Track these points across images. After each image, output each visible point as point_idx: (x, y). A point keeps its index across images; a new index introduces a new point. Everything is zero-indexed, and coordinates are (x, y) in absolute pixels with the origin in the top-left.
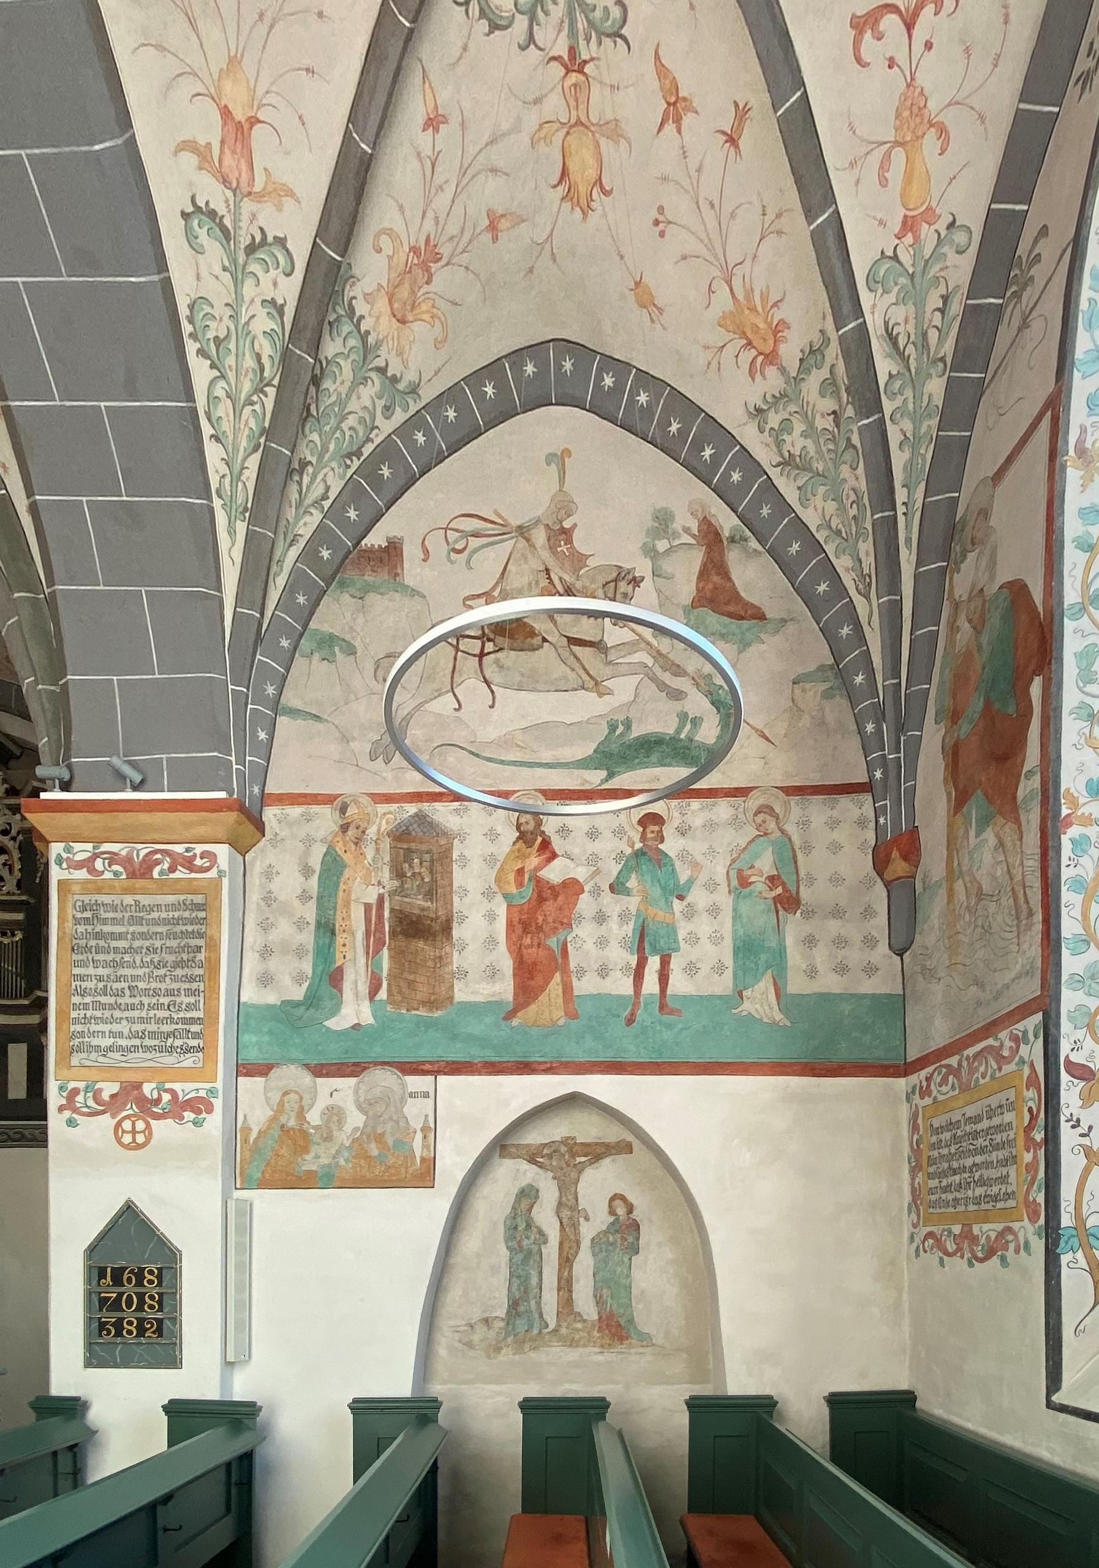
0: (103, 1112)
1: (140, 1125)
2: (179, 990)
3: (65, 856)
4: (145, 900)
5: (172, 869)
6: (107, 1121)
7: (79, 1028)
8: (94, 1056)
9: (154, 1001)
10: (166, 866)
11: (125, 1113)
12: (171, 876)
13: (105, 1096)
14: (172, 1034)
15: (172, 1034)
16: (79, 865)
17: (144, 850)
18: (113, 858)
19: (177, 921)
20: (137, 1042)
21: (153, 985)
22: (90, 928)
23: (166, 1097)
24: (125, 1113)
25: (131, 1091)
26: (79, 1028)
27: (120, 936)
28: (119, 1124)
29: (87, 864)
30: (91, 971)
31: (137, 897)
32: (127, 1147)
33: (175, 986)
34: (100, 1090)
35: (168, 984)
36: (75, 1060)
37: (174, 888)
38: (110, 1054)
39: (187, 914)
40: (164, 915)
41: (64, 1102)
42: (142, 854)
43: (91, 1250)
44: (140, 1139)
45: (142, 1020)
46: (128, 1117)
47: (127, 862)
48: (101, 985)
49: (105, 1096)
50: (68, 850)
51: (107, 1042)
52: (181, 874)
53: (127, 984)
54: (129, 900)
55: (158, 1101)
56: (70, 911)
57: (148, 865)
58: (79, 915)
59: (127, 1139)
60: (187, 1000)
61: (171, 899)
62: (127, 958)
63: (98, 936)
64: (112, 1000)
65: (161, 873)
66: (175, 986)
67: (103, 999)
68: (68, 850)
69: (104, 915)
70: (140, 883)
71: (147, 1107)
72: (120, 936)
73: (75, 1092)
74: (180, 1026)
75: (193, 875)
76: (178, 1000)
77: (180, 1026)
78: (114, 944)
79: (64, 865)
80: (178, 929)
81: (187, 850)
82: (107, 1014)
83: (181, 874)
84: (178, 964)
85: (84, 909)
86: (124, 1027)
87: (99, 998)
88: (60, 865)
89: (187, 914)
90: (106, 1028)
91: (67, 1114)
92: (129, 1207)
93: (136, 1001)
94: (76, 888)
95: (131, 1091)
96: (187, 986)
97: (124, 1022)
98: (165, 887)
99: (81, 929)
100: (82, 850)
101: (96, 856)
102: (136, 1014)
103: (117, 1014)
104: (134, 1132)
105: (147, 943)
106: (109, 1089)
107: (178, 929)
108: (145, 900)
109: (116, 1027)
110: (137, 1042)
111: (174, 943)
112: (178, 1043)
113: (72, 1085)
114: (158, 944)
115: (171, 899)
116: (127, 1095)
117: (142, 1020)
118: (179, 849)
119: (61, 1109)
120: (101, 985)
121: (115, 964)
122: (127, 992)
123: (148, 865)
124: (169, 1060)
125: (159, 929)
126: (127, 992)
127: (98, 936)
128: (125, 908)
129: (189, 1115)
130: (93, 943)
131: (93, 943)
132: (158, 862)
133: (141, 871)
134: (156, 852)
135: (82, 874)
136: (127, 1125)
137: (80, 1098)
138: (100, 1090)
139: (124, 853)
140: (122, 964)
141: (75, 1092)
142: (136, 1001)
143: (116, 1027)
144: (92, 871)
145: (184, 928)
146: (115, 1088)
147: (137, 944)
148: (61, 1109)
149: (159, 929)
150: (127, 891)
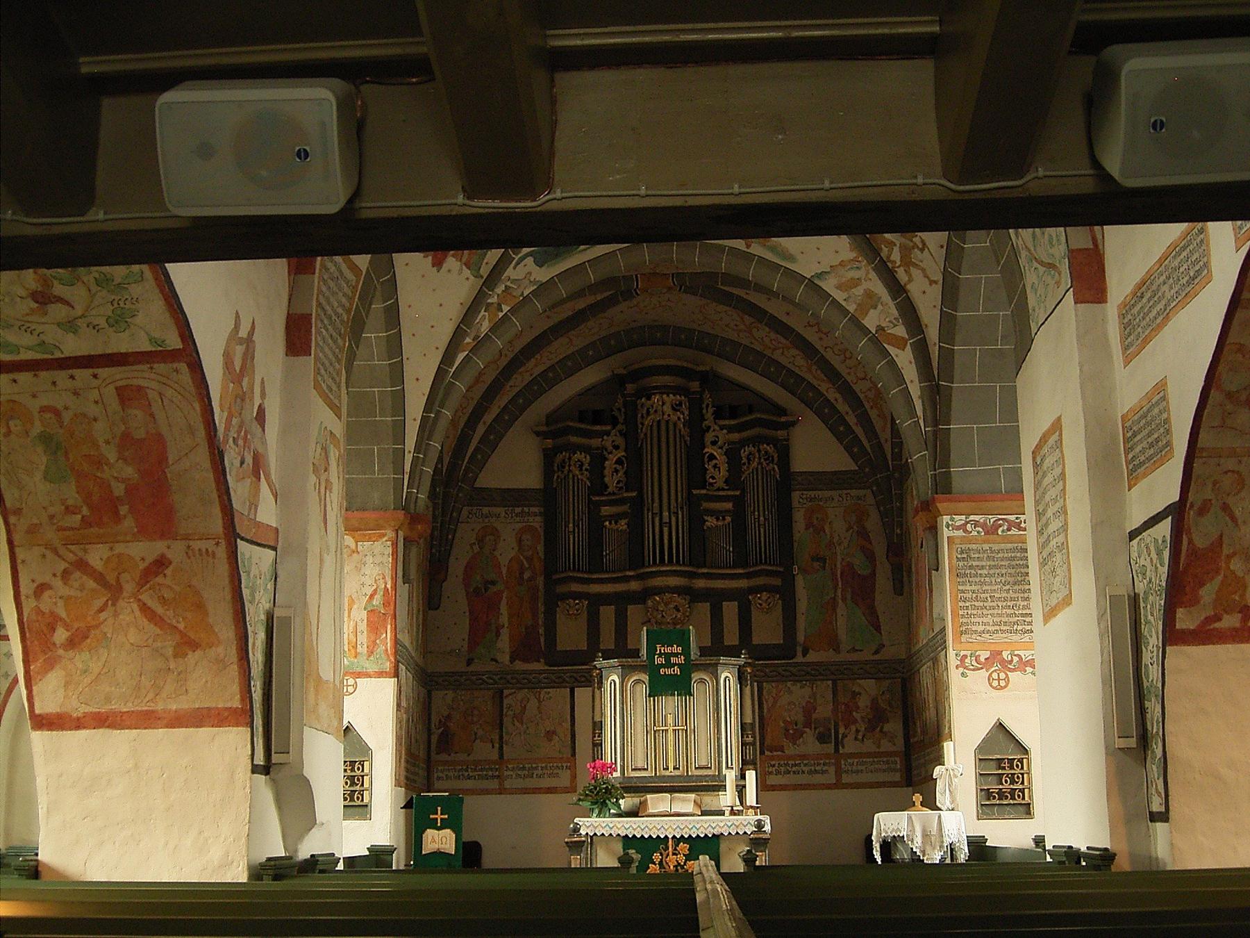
0: (982, 668)
1: (1002, 676)
2: (1018, 598)
3: (950, 523)
4: (995, 547)
5: (1009, 530)
6: (984, 673)
7: (965, 620)
8: (974, 636)
9: (1004, 604)
10: (1005, 528)
11: (993, 669)
12: (1009, 533)
13: (982, 659)
14: (1016, 623)
15: (1016, 623)
16: (958, 528)
17: (992, 519)
18: (976, 524)
19: (1013, 559)
20: (998, 628)
21: (1004, 595)
22: (966, 563)
23: (1016, 659)
24: (993, 669)
25: (996, 655)
26: (965, 620)
27: (983, 567)
28: (990, 675)
29: (963, 527)
30: (968, 588)
31: (990, 545)
32: (995, 688)
33: (1016, 595)
34: (979, 656)
35: (1011, 594)
36: (964, 638)
37: (1007, 539)
38: (983, 635)
39: (1018, 555)
40: (1006, 555)
41: (959, 663)
42: (992, 521)
43: (981, 749)
44: (1003, 683)
45: (999, 615)
46: (995, 671)
47: (984, 526)
48: (974, 595)
49: (982, 659)
50: (952, 520)
51: (981, 628)
52: (1014, 531)
53: (988, 595)
54: (986, 547)
55: (1012, 661)
56: (955, 555)
57: (995, 527)
58: (959, 556)
59: (995, 683)
60: (1022, 604)
61: (1010, 546)
62: (987, 579)
63: (971, 567)
64: (981, 604)
65: (1003, 531)
66: (1016, 595)
67: (976, 604)
68: (952, 520)
69: (973, 556)
70: (991, 537)
71: (1005, 665)
72: (983, 567)
73: (965, 656)
74: (1020, 618)
75: (1022, 533)
76: (1018, 603)
77: (1020, 618)
78: (979, 572)
79: (950, 528)
80: (1014, 563)
81: (1017, 518)
82: (980, 612)
83: (1014, 531)
84: (1015, 584)
85: (962, 552)
86: (989, 619)
87: (973, 603)
88: (948, 528)
89: (1018, 555)
90: (980, 620)
91: (961, 670)
92: (1000, 724)
93: (994, 604)
94: (957, 541)
95: (996, 655)
96: (1022, 595)
97: (989, 616)
98: (1007, 539)
99: (961, 564)
100: (959, 520)
101: (968, 523)
102: (995, 612)
103: (985, 612)
104: (999, 679)
105: (998, 571)
106: (984, 655)
107: (1014, 563)
108: (995, 547)
109: (985, 620)
110: (998, 628)
111: (1013, 571)
112: (1020, 628)
113: (962, 653)
114: (1004, 571)
115: (1010, 546)
116: (994, 659)
117: (999, 615)
118: (1012, 518)
119: (957, 667)
120: (974, 595)
121: (982, 584)
122: (989, 599)
123: (995, 527)
124: (1015, 638)
125: (1003, 563)
126: (989, 599)
127: (971, 567)
128: (984, 552)
129: (1029, 669)
130: (968, 571)
131: (968, 571)
132: (1000, 526)
133: (991, 530)
134: (1000, 519)
135: (960, 533)
136: (995, 676)
137: (967, 660)
138: (979, 656)
139: (981, 521)
140: (985, 583)
141: (965, 656)
142: (994, 604)
143: (985, 620)
144: (965, 531)
145: (1018, 563)
146: (988, 654)
147: (992, 572)
148: (957, 667)
149: (1003, 563)
150: (985, 542)
